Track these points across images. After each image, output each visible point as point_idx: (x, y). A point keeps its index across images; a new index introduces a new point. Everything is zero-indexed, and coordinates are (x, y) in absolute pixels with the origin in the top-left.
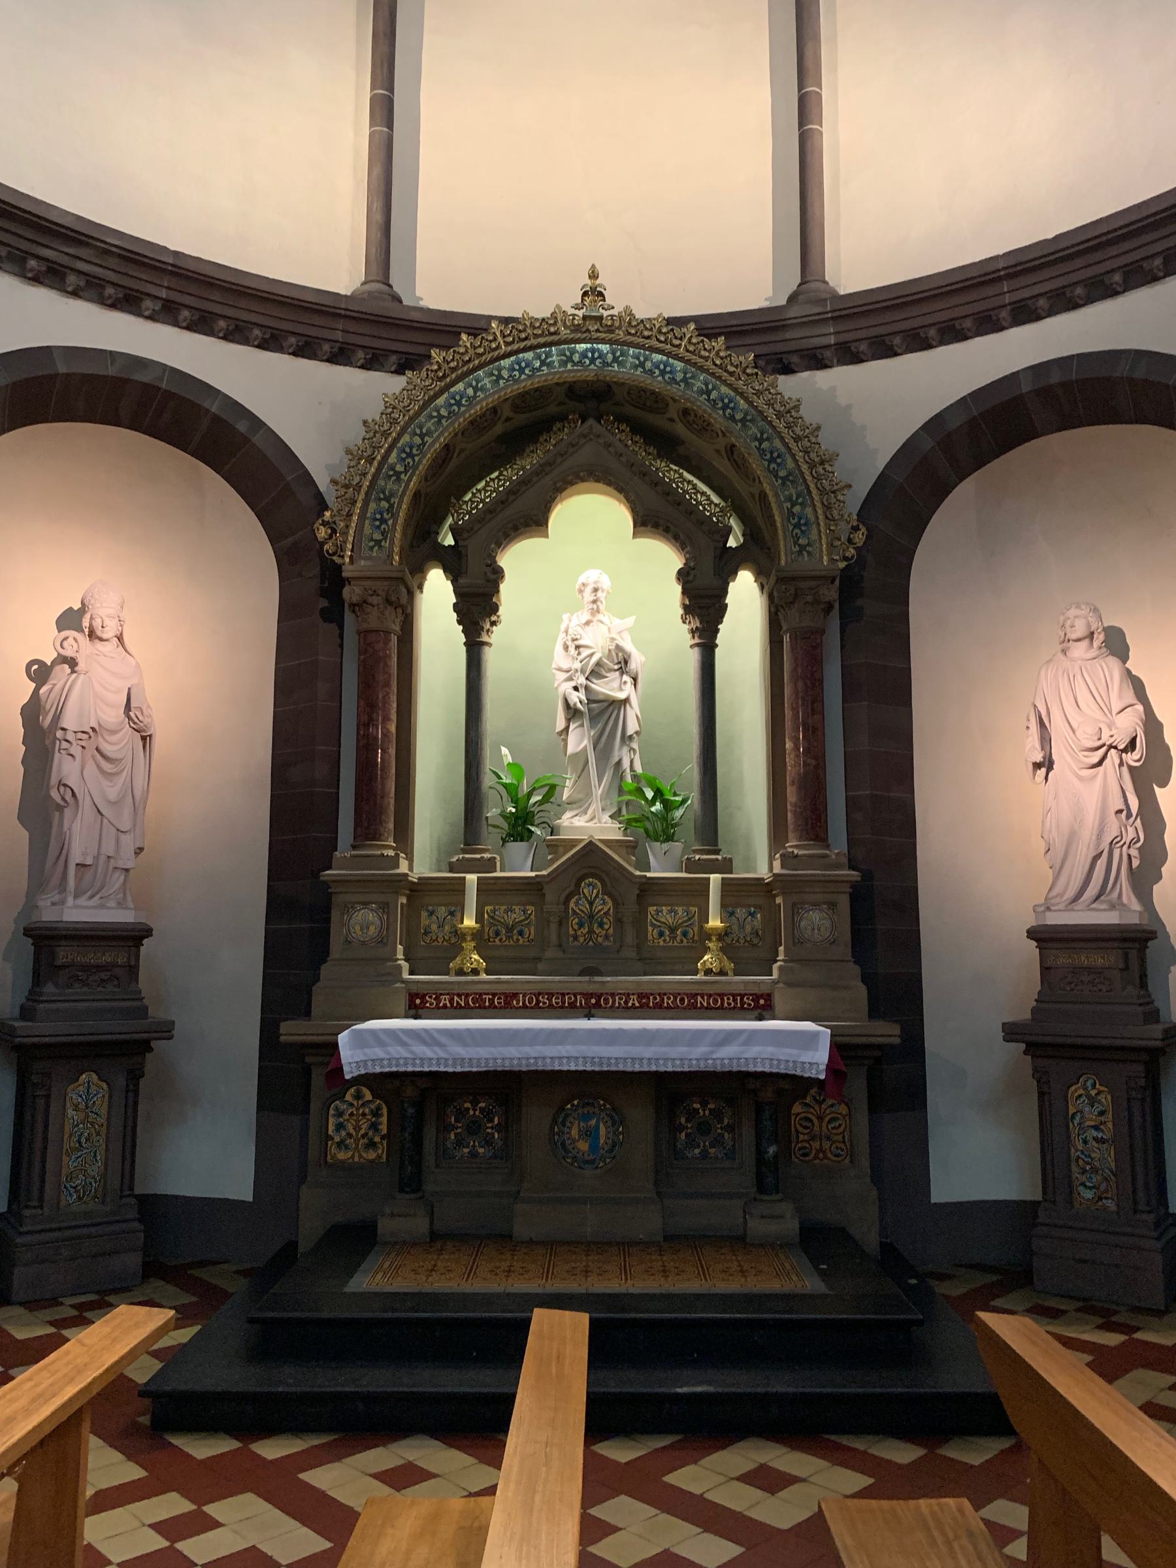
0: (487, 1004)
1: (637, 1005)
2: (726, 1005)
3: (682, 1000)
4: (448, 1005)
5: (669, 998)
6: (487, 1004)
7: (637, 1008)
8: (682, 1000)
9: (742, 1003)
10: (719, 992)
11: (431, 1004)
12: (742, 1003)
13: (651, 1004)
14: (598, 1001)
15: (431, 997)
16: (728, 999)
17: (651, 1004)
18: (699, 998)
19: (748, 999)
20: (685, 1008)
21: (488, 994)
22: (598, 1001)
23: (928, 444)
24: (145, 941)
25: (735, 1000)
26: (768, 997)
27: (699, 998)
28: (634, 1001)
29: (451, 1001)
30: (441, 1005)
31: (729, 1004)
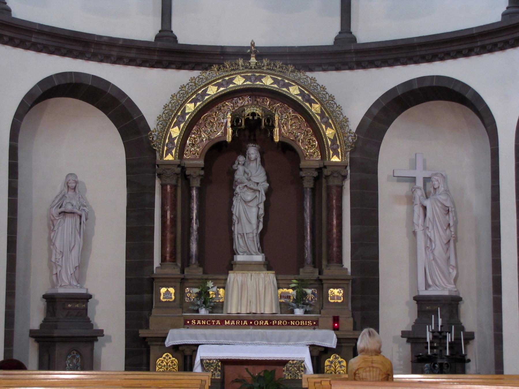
0: (213, 324)
1: (268, 324)
2: (301, 324)
3: (285, 323)
4: (200, 324)
5: (280, 322)
6: (213, 324)
7: (247, 325)
8: (285, 323)
9: (307, 323)
10: (299, 319)
11: (194, 323)
12: (307, 323)
13: (273, 324)
14: (253, 323)
15: (193, 321)
16: (302, 322)
17: (273, 324)
18: (291, 322)
19: (309, 322)
20: (286, 325)
21: (214, 320)
22: (253, 323)
23: (370, 120)
24: (90, 300)
25: (305, 323)
26: (317, 322)
27: (291, 322)
28: (266, 323)
29: (201, 322)
30: (198, 324)
31: (303, 324)
